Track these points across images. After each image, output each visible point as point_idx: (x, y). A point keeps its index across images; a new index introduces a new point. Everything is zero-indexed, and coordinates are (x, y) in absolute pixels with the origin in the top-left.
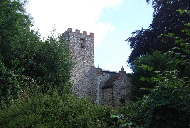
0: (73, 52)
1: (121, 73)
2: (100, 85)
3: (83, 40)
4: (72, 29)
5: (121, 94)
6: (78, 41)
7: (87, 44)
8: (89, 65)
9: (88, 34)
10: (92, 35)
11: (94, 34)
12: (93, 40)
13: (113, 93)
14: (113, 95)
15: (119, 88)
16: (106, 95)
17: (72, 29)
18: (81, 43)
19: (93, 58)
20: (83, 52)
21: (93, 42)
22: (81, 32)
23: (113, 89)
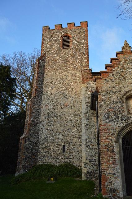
1: (121, 56)
5: (124, 116)
7: (74, 41)
9: (78, 24)
10: (85, 24)
15: (118, 95)
19: (87, 60)
20: (67, 54)
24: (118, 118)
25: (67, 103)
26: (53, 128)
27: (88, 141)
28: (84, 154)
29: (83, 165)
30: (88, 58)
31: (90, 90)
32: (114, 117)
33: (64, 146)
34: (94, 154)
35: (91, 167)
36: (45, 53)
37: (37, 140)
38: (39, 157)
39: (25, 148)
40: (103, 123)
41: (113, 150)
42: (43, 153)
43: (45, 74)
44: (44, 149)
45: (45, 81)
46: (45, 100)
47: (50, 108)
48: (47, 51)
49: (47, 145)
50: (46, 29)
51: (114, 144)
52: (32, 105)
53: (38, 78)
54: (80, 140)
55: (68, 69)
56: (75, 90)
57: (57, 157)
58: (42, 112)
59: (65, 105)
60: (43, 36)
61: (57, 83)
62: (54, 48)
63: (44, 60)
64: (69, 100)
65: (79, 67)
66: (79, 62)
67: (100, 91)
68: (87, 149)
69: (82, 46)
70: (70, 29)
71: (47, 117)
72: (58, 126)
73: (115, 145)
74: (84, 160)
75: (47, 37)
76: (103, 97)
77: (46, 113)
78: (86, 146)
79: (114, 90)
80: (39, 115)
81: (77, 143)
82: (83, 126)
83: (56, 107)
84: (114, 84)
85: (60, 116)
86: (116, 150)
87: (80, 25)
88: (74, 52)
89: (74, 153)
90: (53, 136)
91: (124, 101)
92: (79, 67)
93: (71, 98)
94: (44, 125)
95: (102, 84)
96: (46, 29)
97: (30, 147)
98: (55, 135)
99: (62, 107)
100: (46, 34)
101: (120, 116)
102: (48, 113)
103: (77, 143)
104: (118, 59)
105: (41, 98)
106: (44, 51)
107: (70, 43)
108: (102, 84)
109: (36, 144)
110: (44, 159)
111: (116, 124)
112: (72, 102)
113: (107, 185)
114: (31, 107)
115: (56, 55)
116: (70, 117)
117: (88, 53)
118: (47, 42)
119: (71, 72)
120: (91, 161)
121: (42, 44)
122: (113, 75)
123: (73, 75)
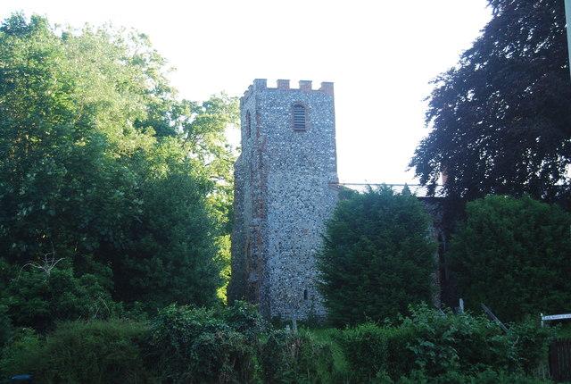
3: (299, 108)
4: (264, 81)
6: (285, 114)
7: (313, 118)
8: (321, 179)
9: (316, 86)
10: (328, 87)
17: (264, 81)
18: (296, 118)
22: (294, 85)
42: (277, 301)
56: (318, 208)
59: (304, 231)
70: (305, 92)
72: (295, 262)
83: (290, 235)
90: (290, 278)
94: (275, 261)
98: (293, 277)
107: (307, 122)
118: (266, 113)
123: (314, 183)
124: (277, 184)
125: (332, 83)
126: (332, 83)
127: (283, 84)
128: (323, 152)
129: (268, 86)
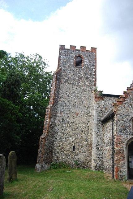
0: (64, 73)
2: (98, 116)
4: (64, 46)
7: (85, 62)
9: (88, 49)
11: (98, 51)
12: (96, 56)
13: (113, 129)
14: (113, 133)
16: (106, 132)
19: (95, 80)
20: (79, 72)
21: (95, 59)
22: (78, 48)
23: (113, 121)
24: (127, 132)
25: (77, 112)
26: (66, 132)
27: (97, 144)
28: (94, 153)
29: (93, 161)
30: (95, 78)
31: (101, 107)
32: (125, 132)
33: (74, 147)
34: (101, 154)
35: (99, 162)
36: (61, 69)
37: (53, 140)
38: (54, 153)
39: (45, 145)
40: (118, 135)
41: (123, 152)
42: (57, 150)
43: (61, 86)
44: (58, 147)
45: (60, 92)
46: (60, 108)
47: (64, 115)
48: (63, 67)
49: (60, 144)
50: (62, 47)
51: (124, 149)
52: (51, 112)
53: (56, 89)
54: (86, 143)
55: (80, 85)
56: (85, 103)
57: (69, 154)
58: (58, 118)
59: (76, 114)
60: (60, 53)
61: (70, 95)
62: (69, 65)
63: (60, 74)
64: (80, 111)
65: (88, 85)
66: (89, 81)
67: (117, 113)
68: (97, 150)
69: (92, 67)
71: (61, 122)
72: (70, 130)
73: (125, 150)
74: (94, 157)
75: (63, 54)
76: (119, 118)
77: (61, 119)
78: (97, 148)
79: (126, 114)
80: (55, 119)
81: (84, 145)
82: (94, 133)
83: (69, 115)
84: (125, 110)
85: (72, 122)
86: (125, 152)
87: (90, 50)
88: (85, 72)
89: (82, 152)
91: (131, 122)
92: (88, 85)
93: (82, 109)
95: (118, 109)
96: (62, 47)
97: (48, 145)
98: (68, 137)
99: (74, 116)
100: (63, 51)
101: (128, 131)
102: (62, 119)
103: (84, 145)
104: (128, 93)
105: (57, 106)
106: (61, 66)
107: (82, 63)
108: (118, 109)
109: (52, 143)
110: (58, 155)
111: (125, 136)
112: (82, 112)
113: (119, 173)
114: (50, 113)
115: (70, 72)
116: (80, 124)
117: (96, 74)
118: (63, 59)
119: (82, 88)
120: (99, 158)
121: (59, 60)
122: (125, 103)
124: (64, 89)
125: (96, 48)
126: (96, 48)
127: (73, 47)
128: (89, 77)
129: (66, 48)
